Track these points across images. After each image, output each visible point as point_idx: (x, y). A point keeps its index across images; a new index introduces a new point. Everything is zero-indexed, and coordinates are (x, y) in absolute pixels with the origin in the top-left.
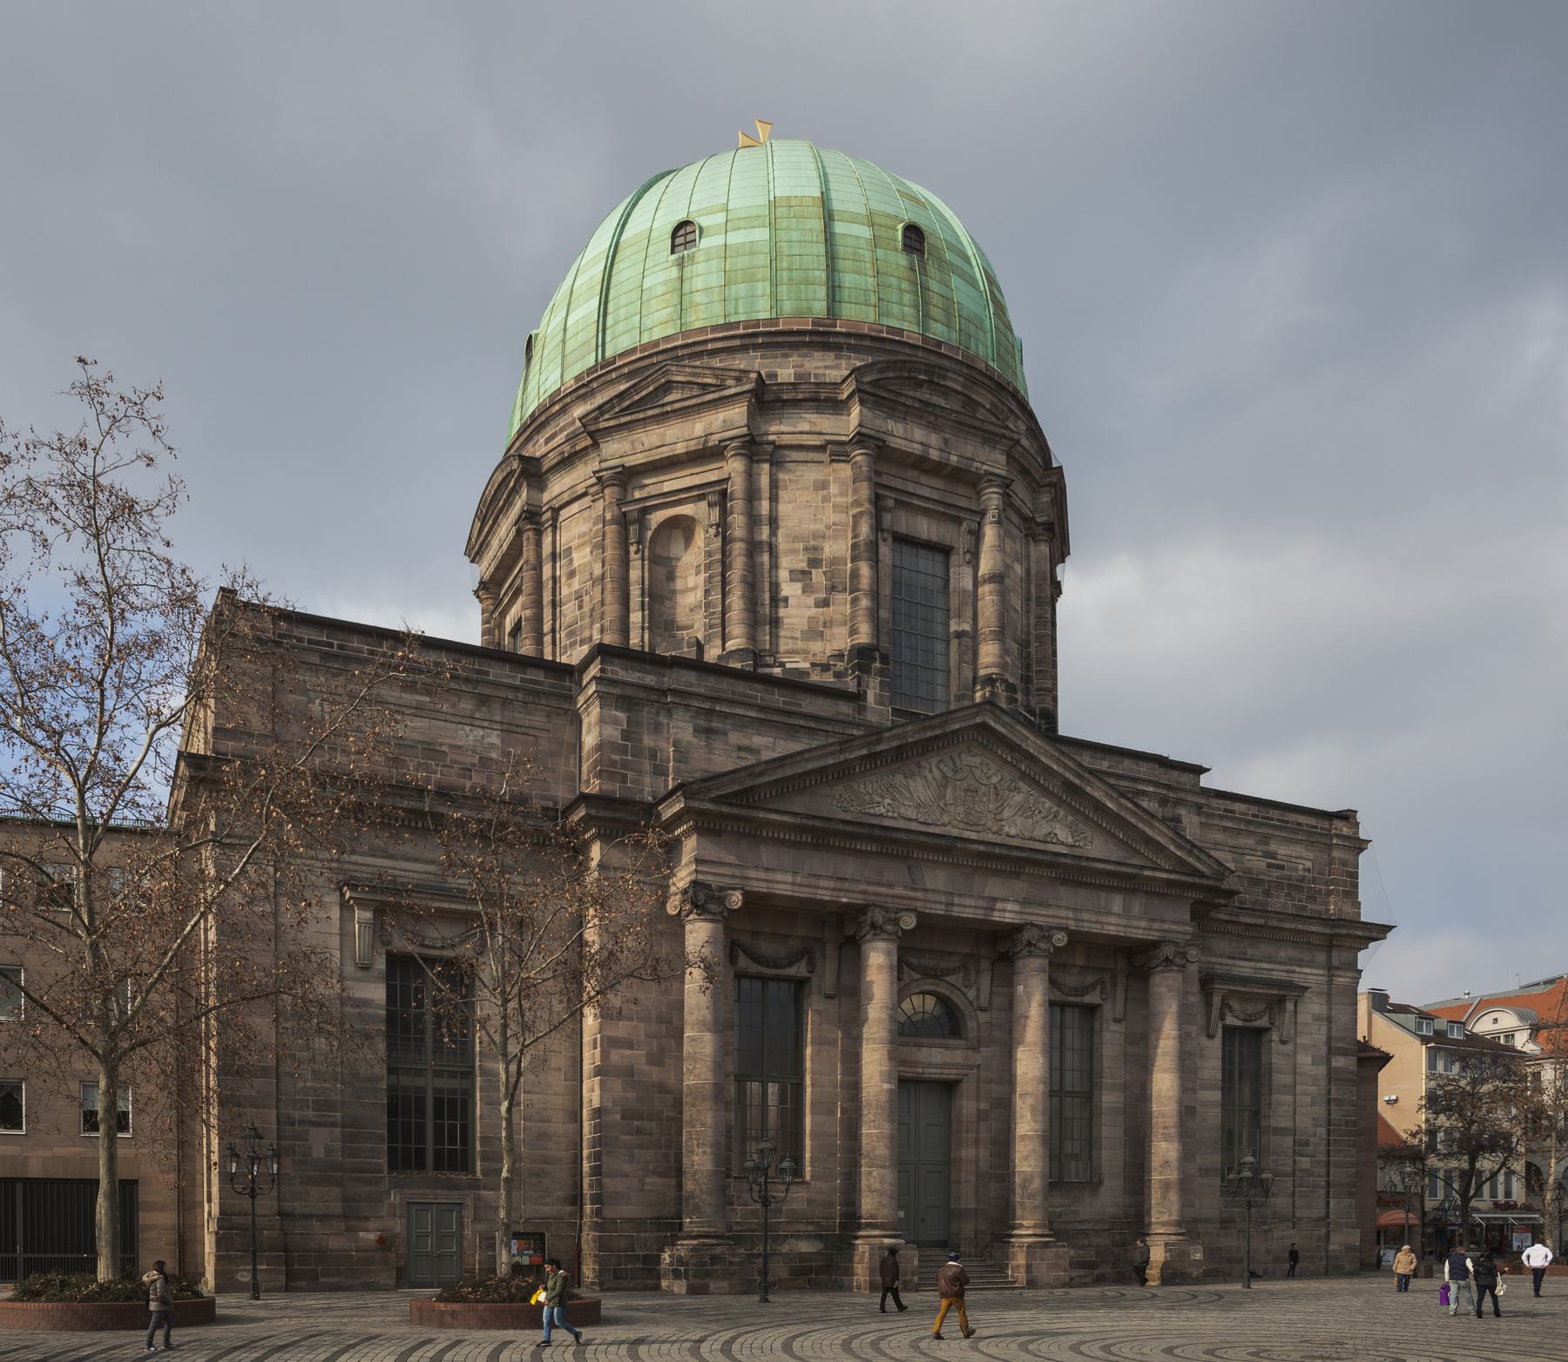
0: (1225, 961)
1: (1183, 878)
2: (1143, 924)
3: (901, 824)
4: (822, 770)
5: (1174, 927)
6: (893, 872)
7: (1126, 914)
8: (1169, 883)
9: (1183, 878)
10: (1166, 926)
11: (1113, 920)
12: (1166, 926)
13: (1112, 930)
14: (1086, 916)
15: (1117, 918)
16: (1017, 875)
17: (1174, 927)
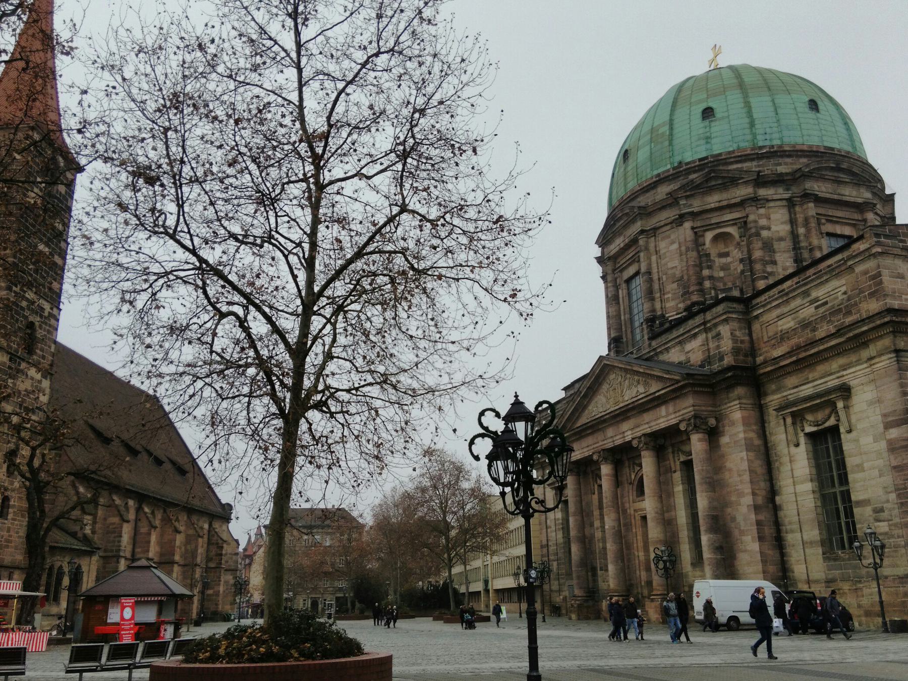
0: (792, 391)
1: (673, 387)
2: (673, 416)
3: (600, 415)
4: (575, 410)
5: (685, 411)
6: (599, 436)
7: (668, 415)
8: (673, 391)
9: (673, 387)
10: (681, 413)
11: (662, 420)
12: (681, 413)
13: (663, 426)
14: (652, 424)
15: (663, 418)
16: (628, 418)
17: (685, 411)
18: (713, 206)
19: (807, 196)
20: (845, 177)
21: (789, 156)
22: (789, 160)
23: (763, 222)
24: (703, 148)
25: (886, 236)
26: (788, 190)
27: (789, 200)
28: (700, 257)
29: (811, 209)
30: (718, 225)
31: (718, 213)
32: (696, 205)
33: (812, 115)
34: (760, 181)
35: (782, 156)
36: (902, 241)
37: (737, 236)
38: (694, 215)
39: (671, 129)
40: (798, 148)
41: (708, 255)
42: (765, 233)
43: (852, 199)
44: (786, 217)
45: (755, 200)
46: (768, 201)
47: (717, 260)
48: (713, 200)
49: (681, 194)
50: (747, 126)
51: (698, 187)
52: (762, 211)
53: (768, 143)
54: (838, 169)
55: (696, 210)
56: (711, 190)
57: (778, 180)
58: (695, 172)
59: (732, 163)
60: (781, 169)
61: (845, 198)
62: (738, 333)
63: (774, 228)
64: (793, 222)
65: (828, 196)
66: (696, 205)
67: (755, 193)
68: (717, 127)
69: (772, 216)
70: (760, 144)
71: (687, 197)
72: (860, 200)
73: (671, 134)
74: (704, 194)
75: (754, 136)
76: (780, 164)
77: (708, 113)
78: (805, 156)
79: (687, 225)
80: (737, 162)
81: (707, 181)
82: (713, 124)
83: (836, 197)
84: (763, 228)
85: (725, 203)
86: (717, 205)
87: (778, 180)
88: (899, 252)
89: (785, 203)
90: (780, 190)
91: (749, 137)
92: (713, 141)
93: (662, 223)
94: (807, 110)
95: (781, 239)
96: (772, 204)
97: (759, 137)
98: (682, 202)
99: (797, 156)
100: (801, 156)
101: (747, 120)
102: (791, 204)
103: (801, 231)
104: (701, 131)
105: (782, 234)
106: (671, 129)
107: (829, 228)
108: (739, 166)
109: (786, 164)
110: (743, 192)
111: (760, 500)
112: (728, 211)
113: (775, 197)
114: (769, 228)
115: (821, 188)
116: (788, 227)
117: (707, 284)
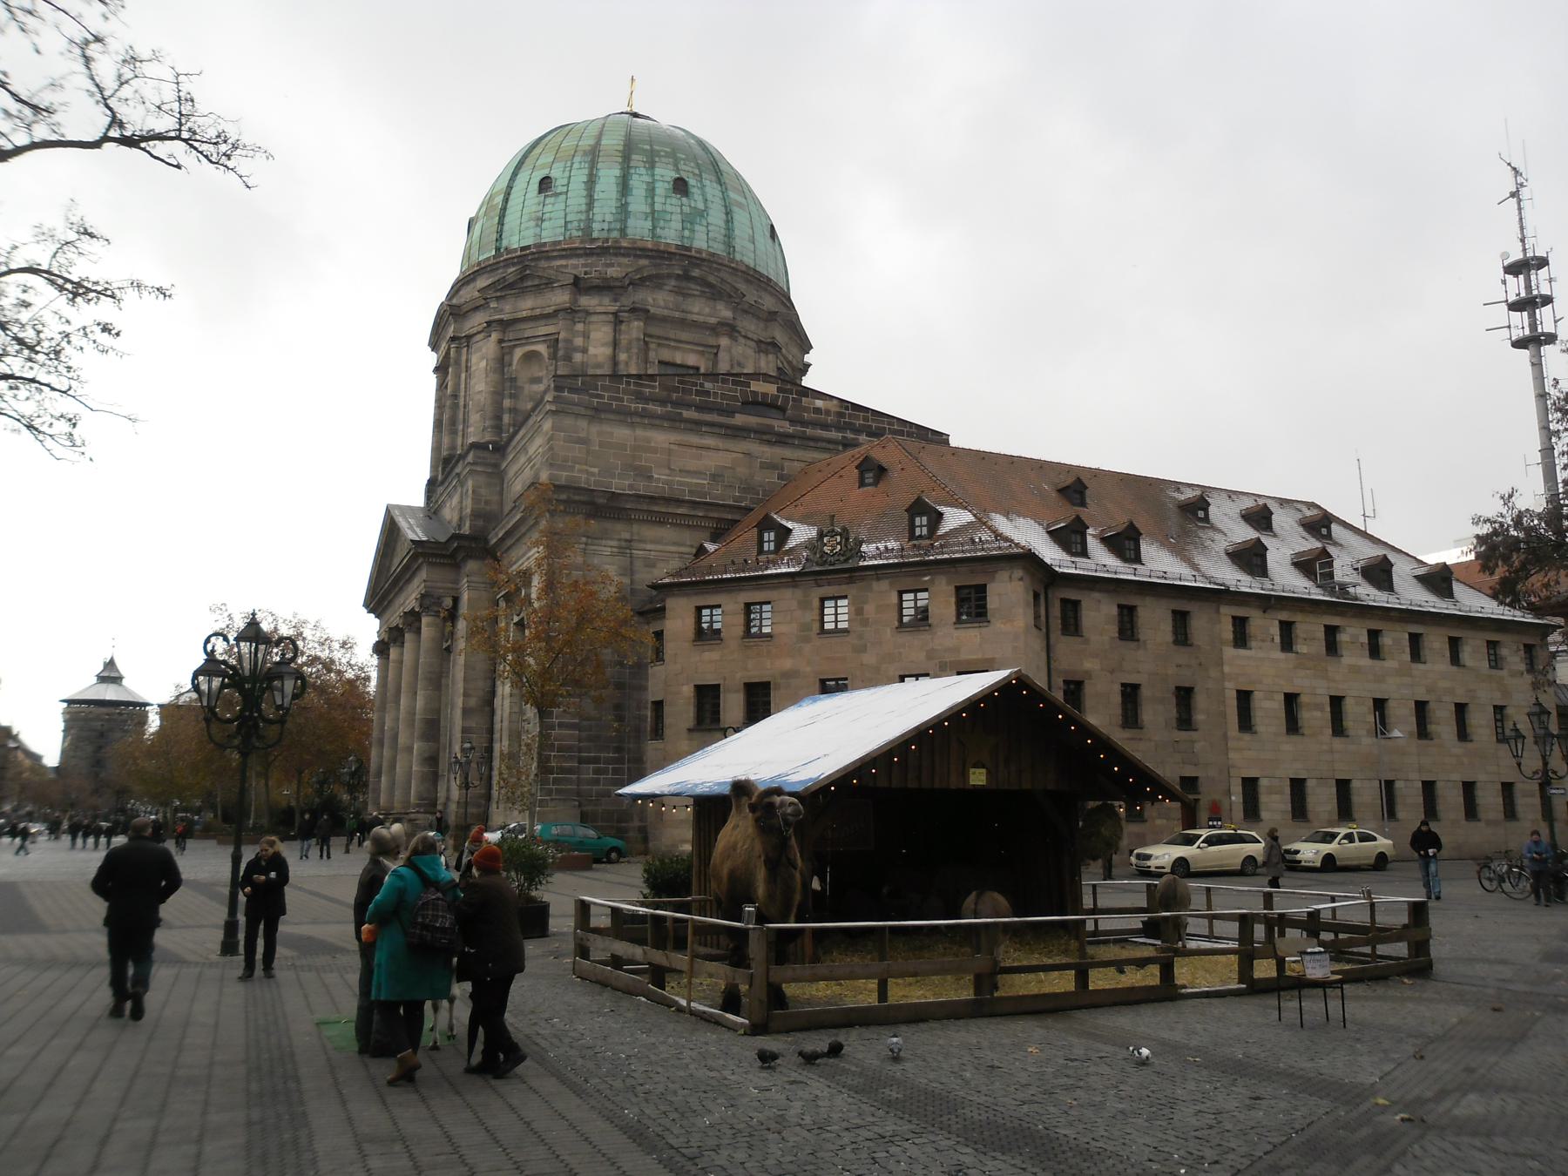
18: (524, 314)
19: (638, 311)
20: (695, 288)
21: (628, 255)
22: (625, 260)
23: (579, 341)
24: (531, 232)
25: (571, 390)
26: (616, 300)
27: (615, 314)
28: (503, 381)
29: (635, 328)
30: (528, 340)
31: (531, 324)
32: (507, 309)
34: (578, 286)
35: (616, 255)
36: (598, 396)
37: (546, 355)
38: (504, 325)
39: (506, 200)
40: (639, 244)
41: (513, 380)
42: (578, 357)
43: (701, 319)
44: (610, 338)
45: (572, 312)
46: (588, 313)
47: (527, 386)
48: (527, 305)
49: (490, 294)
50: (584, 208)
51: (511, 286)
52: (580, 327)
53: (605, 234)
54: (686, 277)
55: (505, 317)
56: (523, 292)
57: (605, 287)
58: (514, 264)
59: (555, 258)
60: (612, 272)
61: (690, 317)
62: (483, 491)
63: (592, 351)
64: (615, 344)
65: (666, 312)
66: (507, 309)
68: (554, 207)
69: (593, 335)
70: (595, 235)
71: (498, 298)
72: (713, 320)
73: (504, 209)
74: (517, 296)
75: (589, 221)
76: (612, 265)
77: (545, 184)
78: (647, 257)
79: (494, 336)
80: (562, 257)
81: (522, 279)
82: (549, 200)
83: (677, 315)
84: (576, 350)
85: (538, 312)
86: (529, 313)
87: (605, 287)
88: (583, 411)
89: (611, 317)
90: (606, 301)
92: (545, 225)
93: (474, 330)
96: (594, 318)
97: (596, 226)
98: (493, 305)
99: (636, 256)
100: (640, 257)
102: (617, 320)
104: (534, 208)
105: (601, 359)
106: (506, 200)
107: (666, 355)
108: (563, 262)
109: (619, 265)
110: (561, 298)
111: (473, 702)
112: (543, 322)
113: (599, 309)
114: (585, 351)
115: (658, 300)
116: (608, 351)
117: (506, 418)
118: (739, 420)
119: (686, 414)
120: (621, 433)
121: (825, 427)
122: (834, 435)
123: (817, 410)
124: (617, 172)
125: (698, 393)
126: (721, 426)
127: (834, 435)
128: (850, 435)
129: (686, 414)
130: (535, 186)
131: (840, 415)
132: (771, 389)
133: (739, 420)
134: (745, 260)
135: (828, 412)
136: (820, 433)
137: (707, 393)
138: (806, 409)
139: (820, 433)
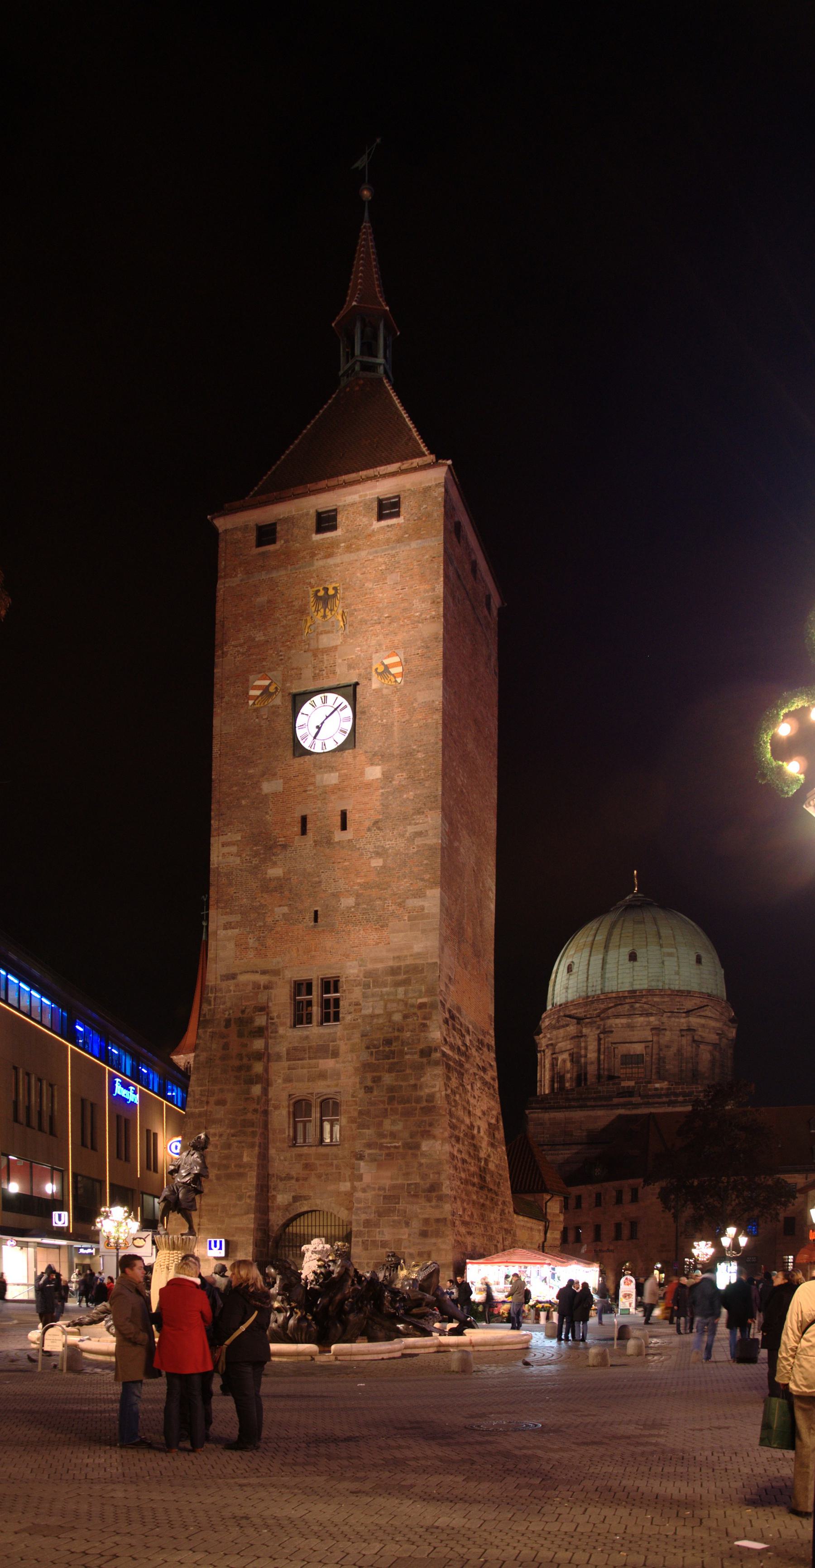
23: (583, 1052)
24: (564, 996)
33: (630, 964)
40: (610, 995)
42: (583, 1060)
44: (596, 1048)
53: (593, 993)
63: (589, 1055)
67: (581, 1032)
69: (589, 1048)
70: (589, 994)
82: (571, 977)
91: (585, 988)
94: (627, 961)
95: (592, 1063)
97: (590, 989)
101: (585, 976)
103: (602, 1057)
114: (586, 1056)
116: (595, 1055)
118: (615, 1101)
119: (589, 1103)
120: (560, 1115)
121: (660, 1096)
122: (665, 1099)
123: (656, 1089)
124: (601, 956)
125: (595, 1093)
126: (607, 1106)
127: (665, 1099)
128: (673, 1098)
129: (589, 1103)
130: (566, 970)
131: (668, 1089)
132: (632, 1083)
133: (615, 1101)
134: (672, 987)
135: (662, 1089)
136: (656, 1100)
137: (600, 1092)
138: (650, 1090)
139: (656, 1100)
